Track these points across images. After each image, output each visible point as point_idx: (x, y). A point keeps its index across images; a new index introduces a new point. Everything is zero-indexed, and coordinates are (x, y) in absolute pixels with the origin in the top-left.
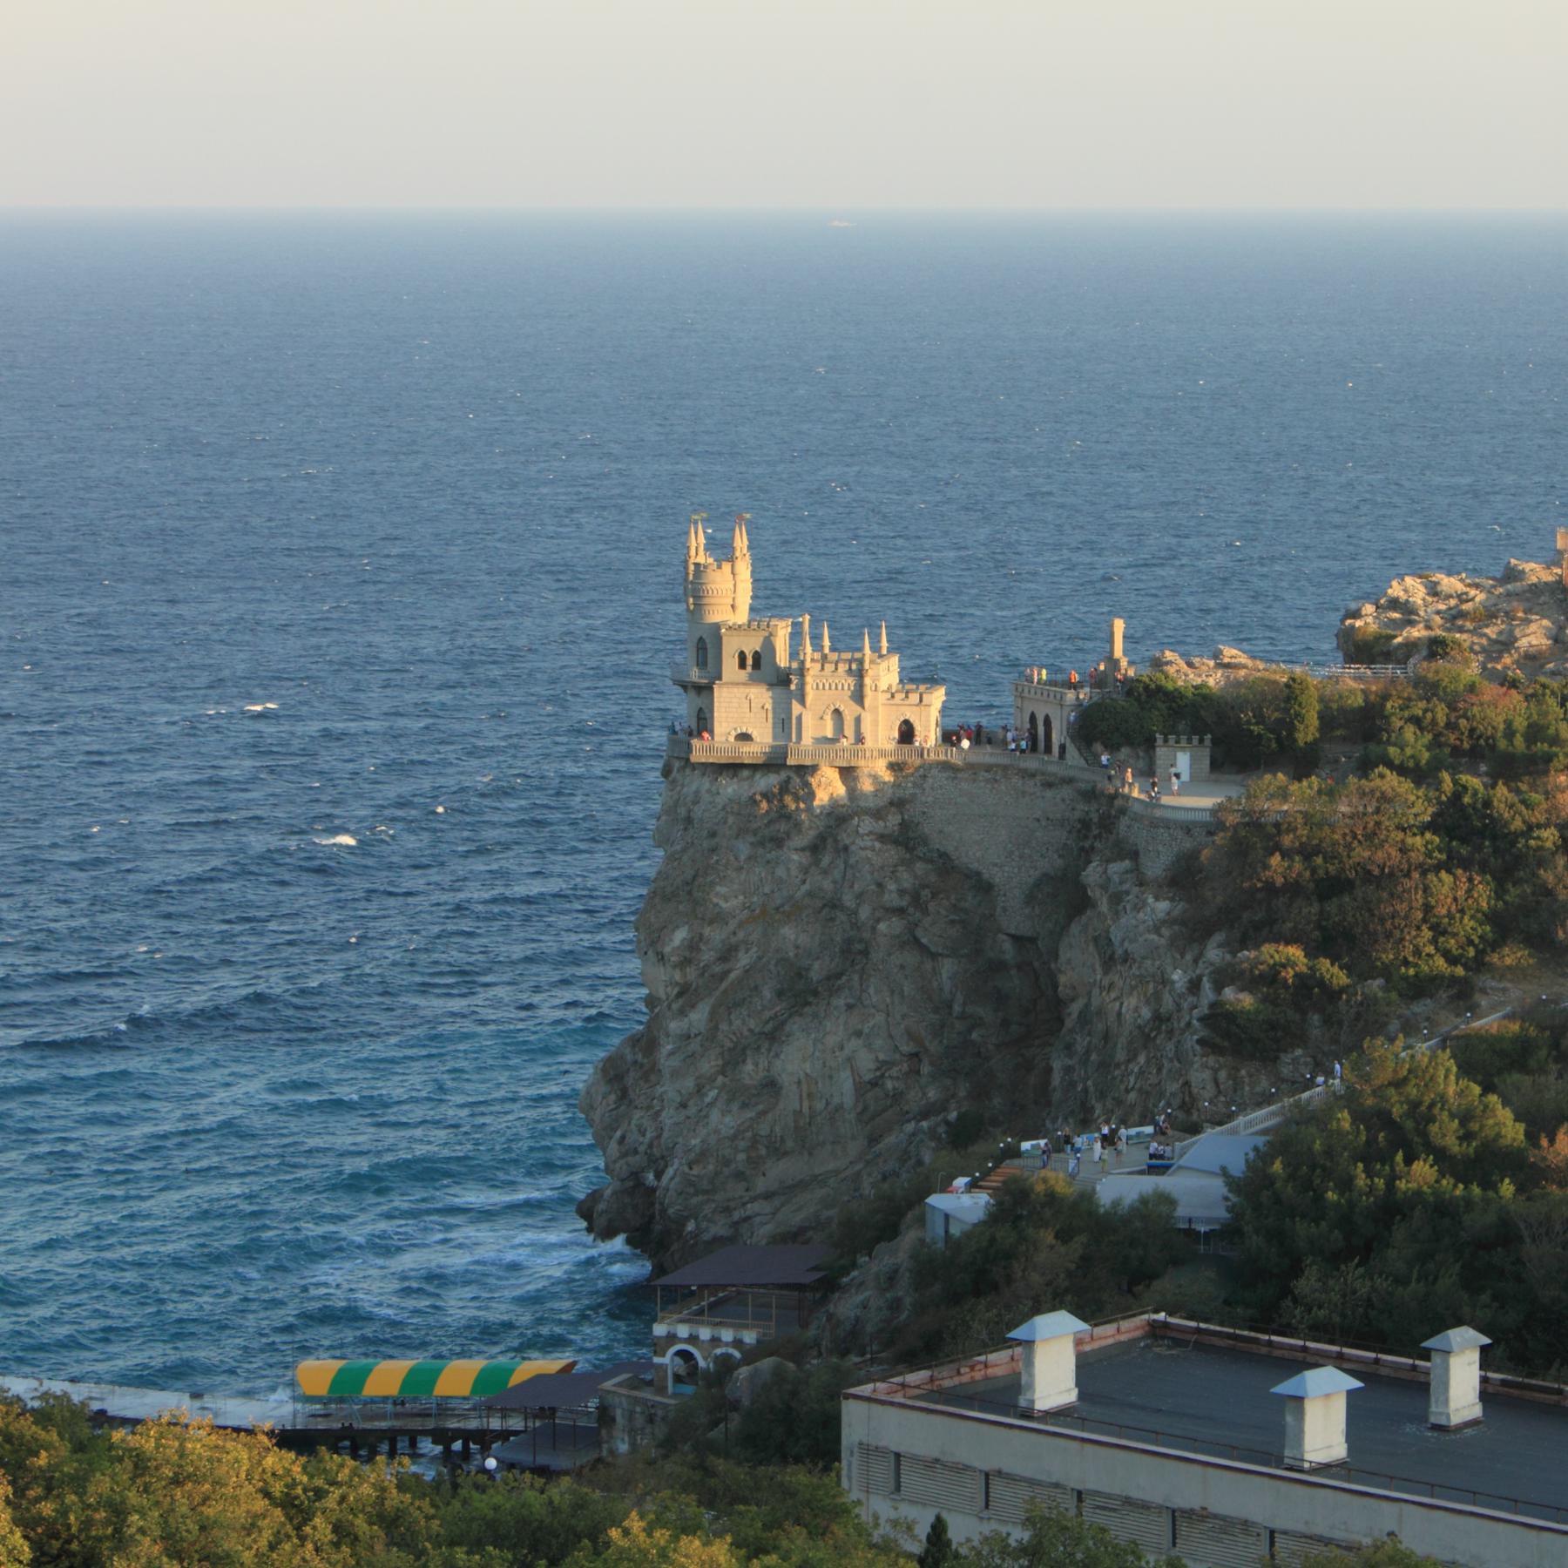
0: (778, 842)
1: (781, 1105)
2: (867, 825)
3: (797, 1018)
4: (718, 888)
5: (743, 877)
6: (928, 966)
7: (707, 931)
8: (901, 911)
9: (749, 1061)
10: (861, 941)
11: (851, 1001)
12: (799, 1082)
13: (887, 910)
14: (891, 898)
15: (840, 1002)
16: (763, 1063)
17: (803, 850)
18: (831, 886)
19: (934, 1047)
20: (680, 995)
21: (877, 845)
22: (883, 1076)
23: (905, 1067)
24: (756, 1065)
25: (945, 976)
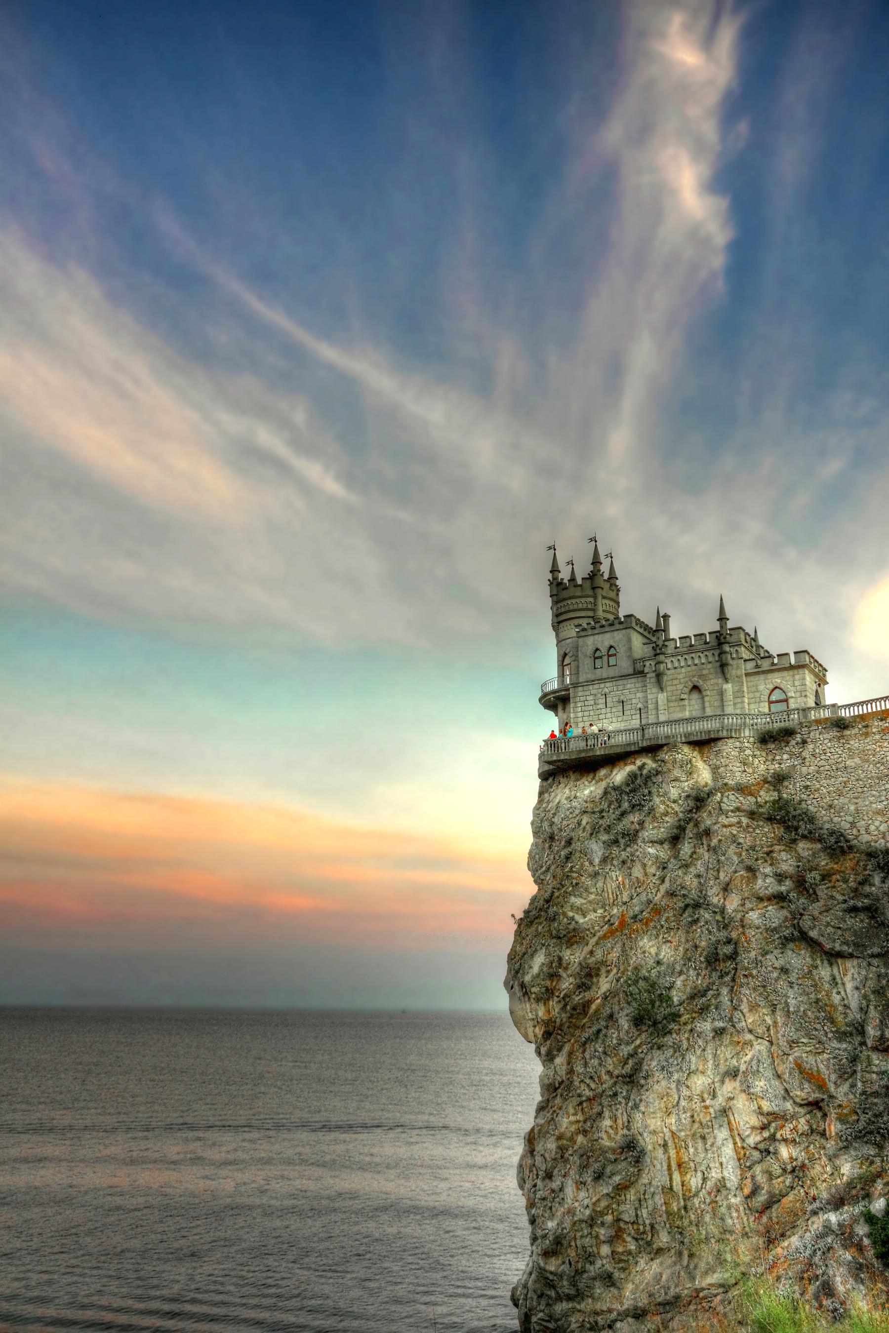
0: (632, 837)
1: (644, 1180)
2: (731, 801)
3: (656, 1053)
4: (573, 899)
5: (600, 884)
6: (824, 972)
7: (566, 954)
8: (780, 898)
9: (607, 1114)
10: (729, 941)
11: (720, 1024)
12: (665, 1145)
13: (760, 899)
14: (766, 884)
15: (706, 1026)
16: (622, 1119)
17: (661, 843)
18: (696, 881)
19: (842, 1093)
20: (547, 1035)
21: (745, 821)
22: (773, 1138)
23: (802, 1124)
24: (615, 1119)
25: (849, 986)
